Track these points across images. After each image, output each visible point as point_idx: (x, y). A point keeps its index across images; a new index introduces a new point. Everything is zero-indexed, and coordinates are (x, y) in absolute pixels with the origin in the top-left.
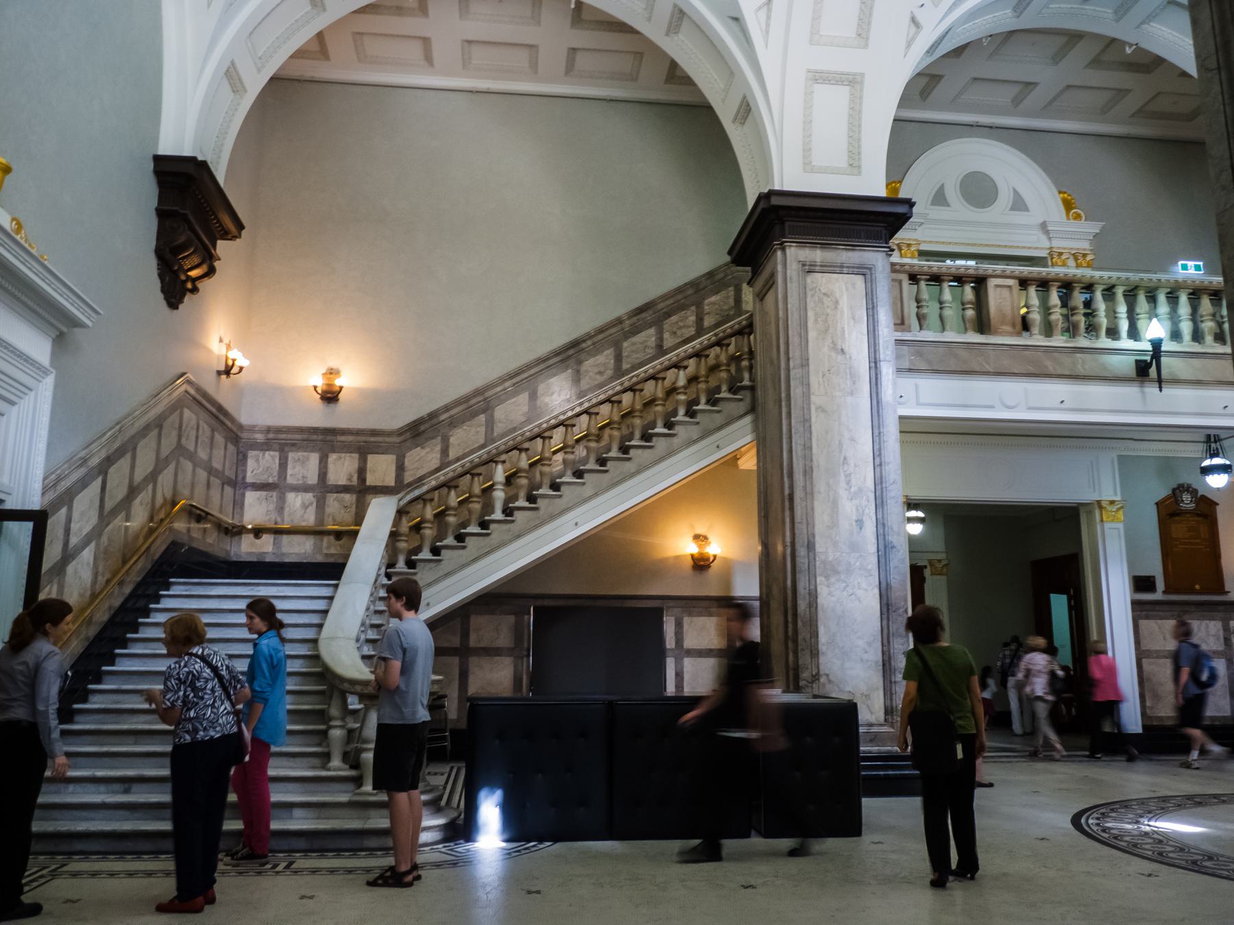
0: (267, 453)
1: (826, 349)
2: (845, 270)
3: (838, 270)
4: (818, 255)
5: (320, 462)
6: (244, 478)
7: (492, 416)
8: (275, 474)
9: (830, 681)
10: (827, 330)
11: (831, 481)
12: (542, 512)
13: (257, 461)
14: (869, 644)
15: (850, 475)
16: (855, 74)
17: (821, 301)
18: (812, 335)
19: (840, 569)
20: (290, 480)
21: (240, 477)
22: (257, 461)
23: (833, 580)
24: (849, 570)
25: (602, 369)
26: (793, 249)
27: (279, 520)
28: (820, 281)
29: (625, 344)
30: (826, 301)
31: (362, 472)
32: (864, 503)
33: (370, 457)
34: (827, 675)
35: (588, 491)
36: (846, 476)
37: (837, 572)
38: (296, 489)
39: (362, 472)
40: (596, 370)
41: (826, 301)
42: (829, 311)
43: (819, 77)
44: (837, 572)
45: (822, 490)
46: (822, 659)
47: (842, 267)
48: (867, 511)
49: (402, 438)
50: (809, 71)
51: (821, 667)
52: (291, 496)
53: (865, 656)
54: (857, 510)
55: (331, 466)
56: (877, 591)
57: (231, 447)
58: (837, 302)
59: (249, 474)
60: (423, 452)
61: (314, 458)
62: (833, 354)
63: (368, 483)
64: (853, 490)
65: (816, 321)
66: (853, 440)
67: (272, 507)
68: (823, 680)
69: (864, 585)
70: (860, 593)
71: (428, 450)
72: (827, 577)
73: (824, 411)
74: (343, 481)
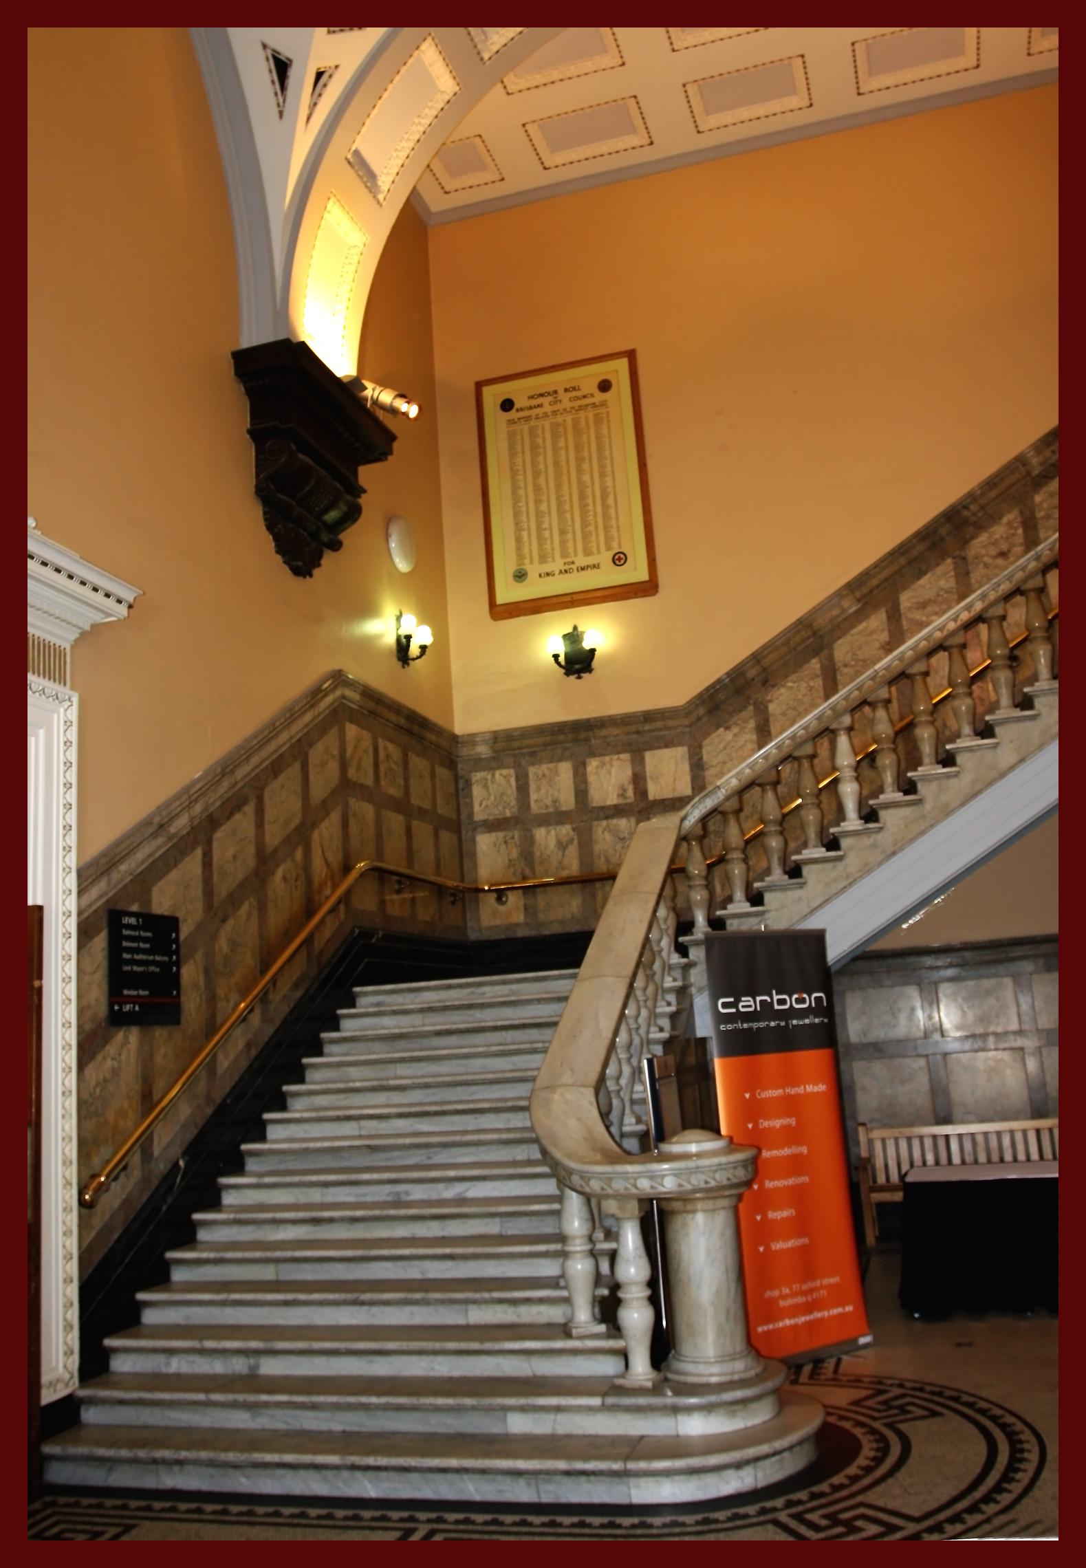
0: (497, 773)
5: (576, 773)
6: (471, 814)
7: (831, 657)
8: (513, 802)
13: (486, 787)
20: (535, 809)
21: (463, 817)
22: (486, 787)
25: (1004, 547)
27: (527, 872)
29: (1038, 499)
31: (639, 780)
33: (648, 756)
35: (1006, 755)
38: (545, 820)
39: (639, 780)
40: (993, 552)
49: (693, 717)
52: (540, 833)
55: (591, 778)
57: (442, 772)
59: (476, 808)
60: (729, 736)
61: (565, 770)
63: (651, 797)
67: (515, 853)
71: (735, 730)
74: (612, 800)
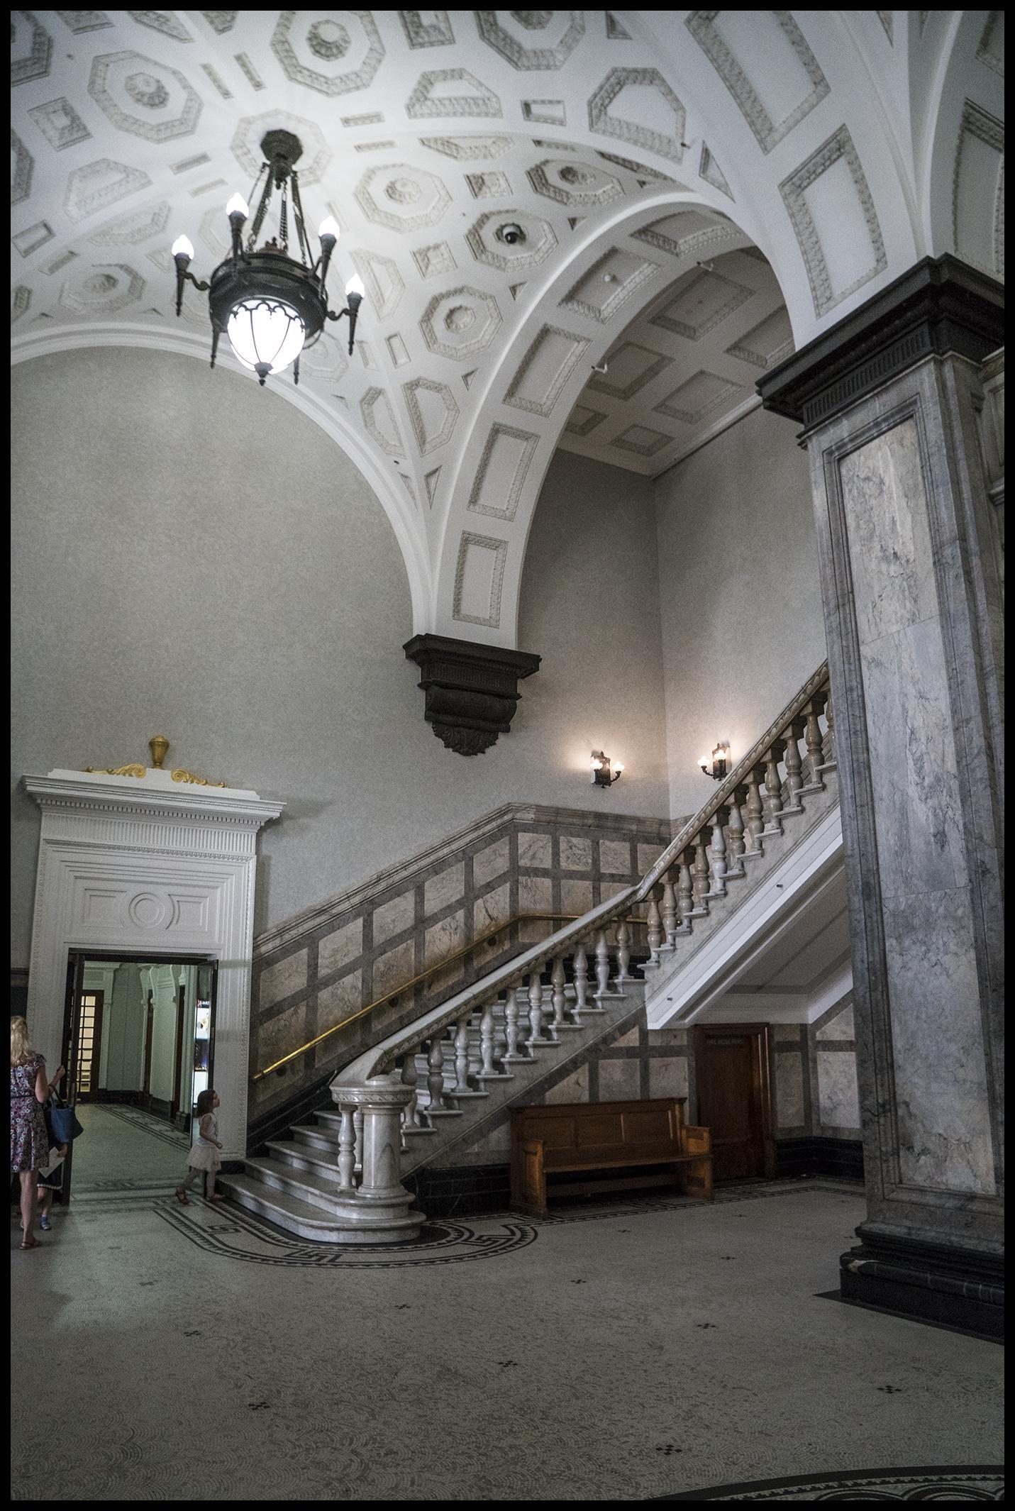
1: (873, 565)
2: (884, 426)
3: (874, 432)
4: (843, 429)
9: (910, 1115)
10: (871, 536)
11: (896, 777)
12: (749, 877)
14: (966, 1051)
15: (921, 758)
16: (835, 136)
17: (862, 493)
18: (855, 549)
19: (916, 922)
23: (907, 943)
24: (929, 925)
26: (814, 439)
28: (858, 464)
30: (870, 489)
32: (945, 799)
34: (907, 1104)
36: (916, 761)
37: (911, 928)
41: (870, 489)
42: (873, 502)
43: (797, 183)
44: (911, 928)
45: (885, 795)
46: (900, 1077)
47: (877, 424)
48: (950, 813)
50: (782, 185)
51: (899, 1091)
53: (961, 1073)
54: (935, 816)
56: (972, 954)
58: (882, 482)
62: (884, 567)
64: (926, 783)
65: (858, 526)
66: (921, 696)
68: (900, 1112)
69: (953, 947)
70: (948, 960)
72: (899, 938)
73: (879, 664)
